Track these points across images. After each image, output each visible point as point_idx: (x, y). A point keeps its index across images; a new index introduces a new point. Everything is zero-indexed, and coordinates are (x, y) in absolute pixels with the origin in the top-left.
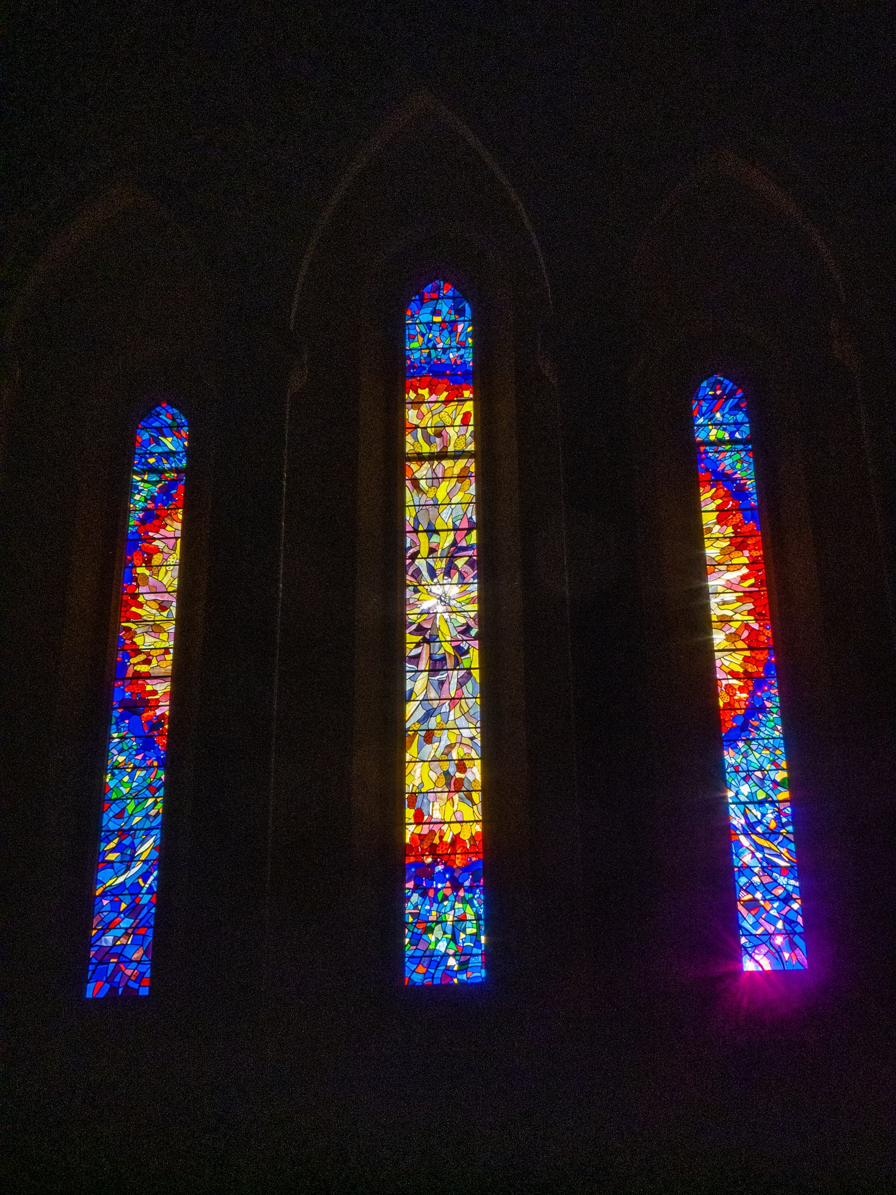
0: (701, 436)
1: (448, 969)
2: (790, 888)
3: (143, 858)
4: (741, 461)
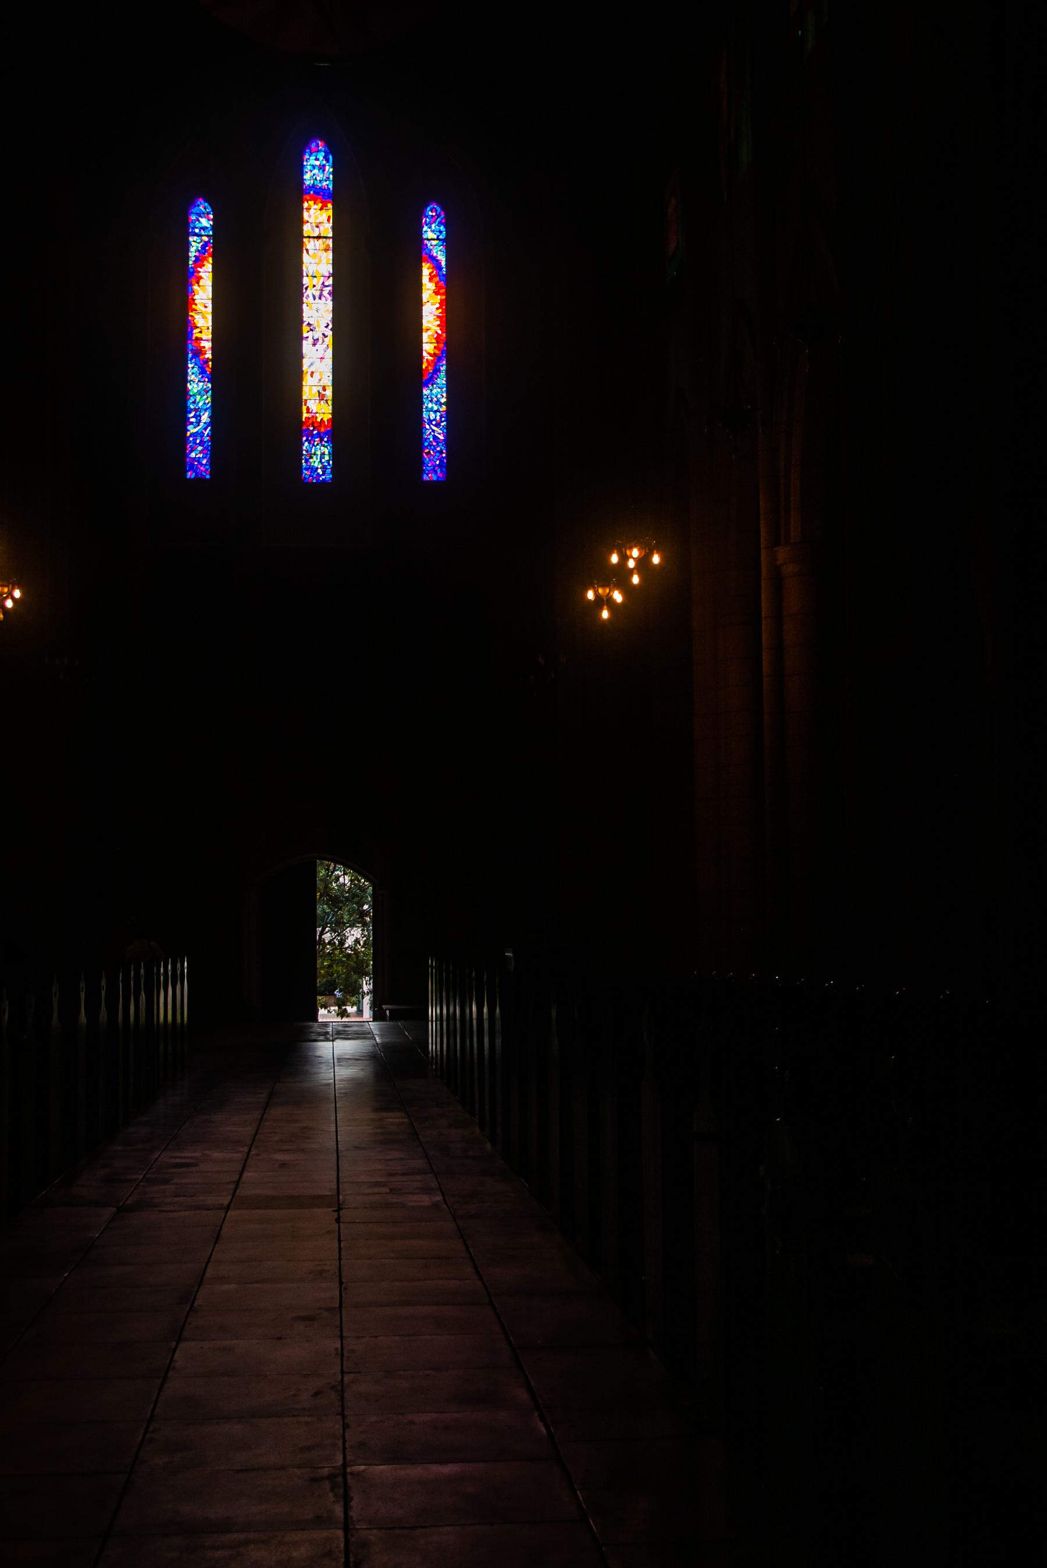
0: (425, 236)
1: (318, 474)
2: (443, 448)
3: (204, 421)
4: (440, 251)
